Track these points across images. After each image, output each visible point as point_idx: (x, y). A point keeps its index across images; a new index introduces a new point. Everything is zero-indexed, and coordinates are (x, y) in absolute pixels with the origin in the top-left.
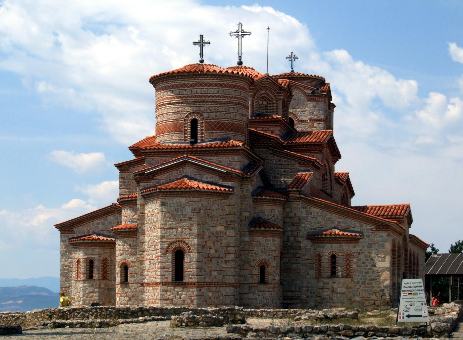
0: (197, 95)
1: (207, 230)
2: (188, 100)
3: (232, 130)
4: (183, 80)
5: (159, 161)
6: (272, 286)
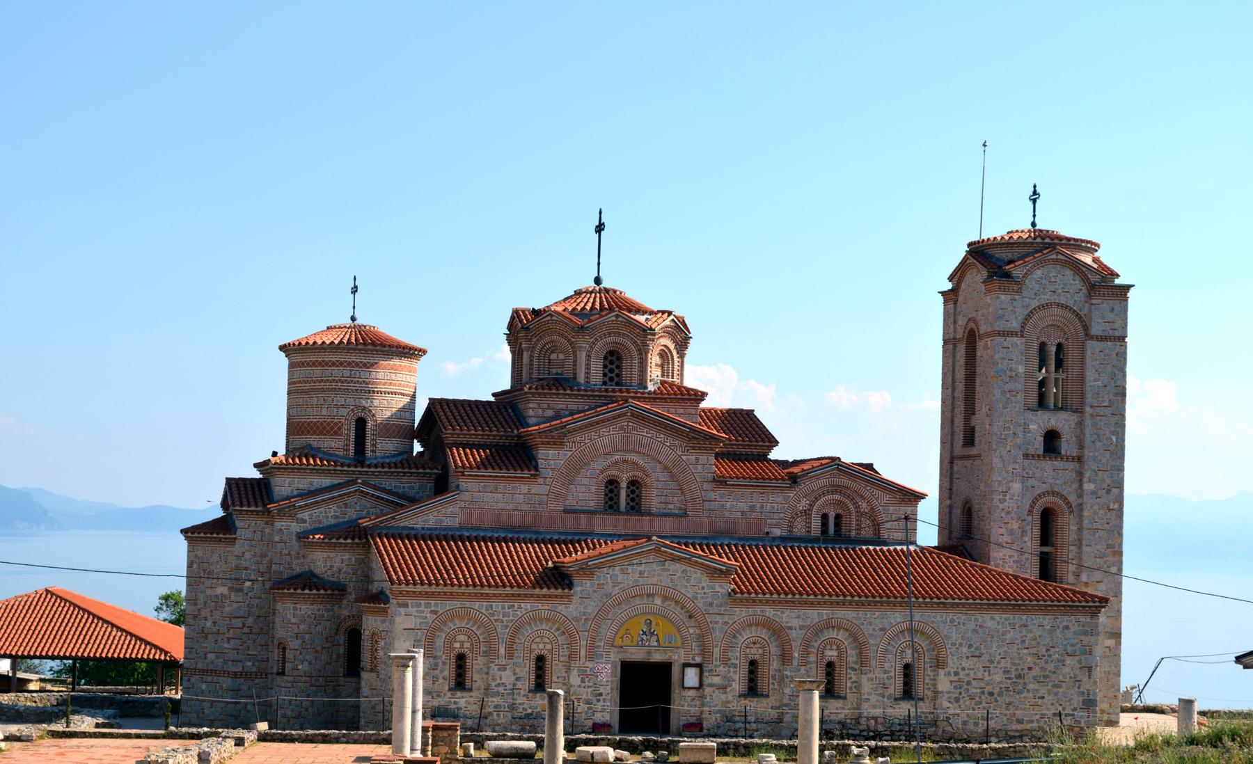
1: (202, 592)
3: (315, 433)
6: (291, 679)
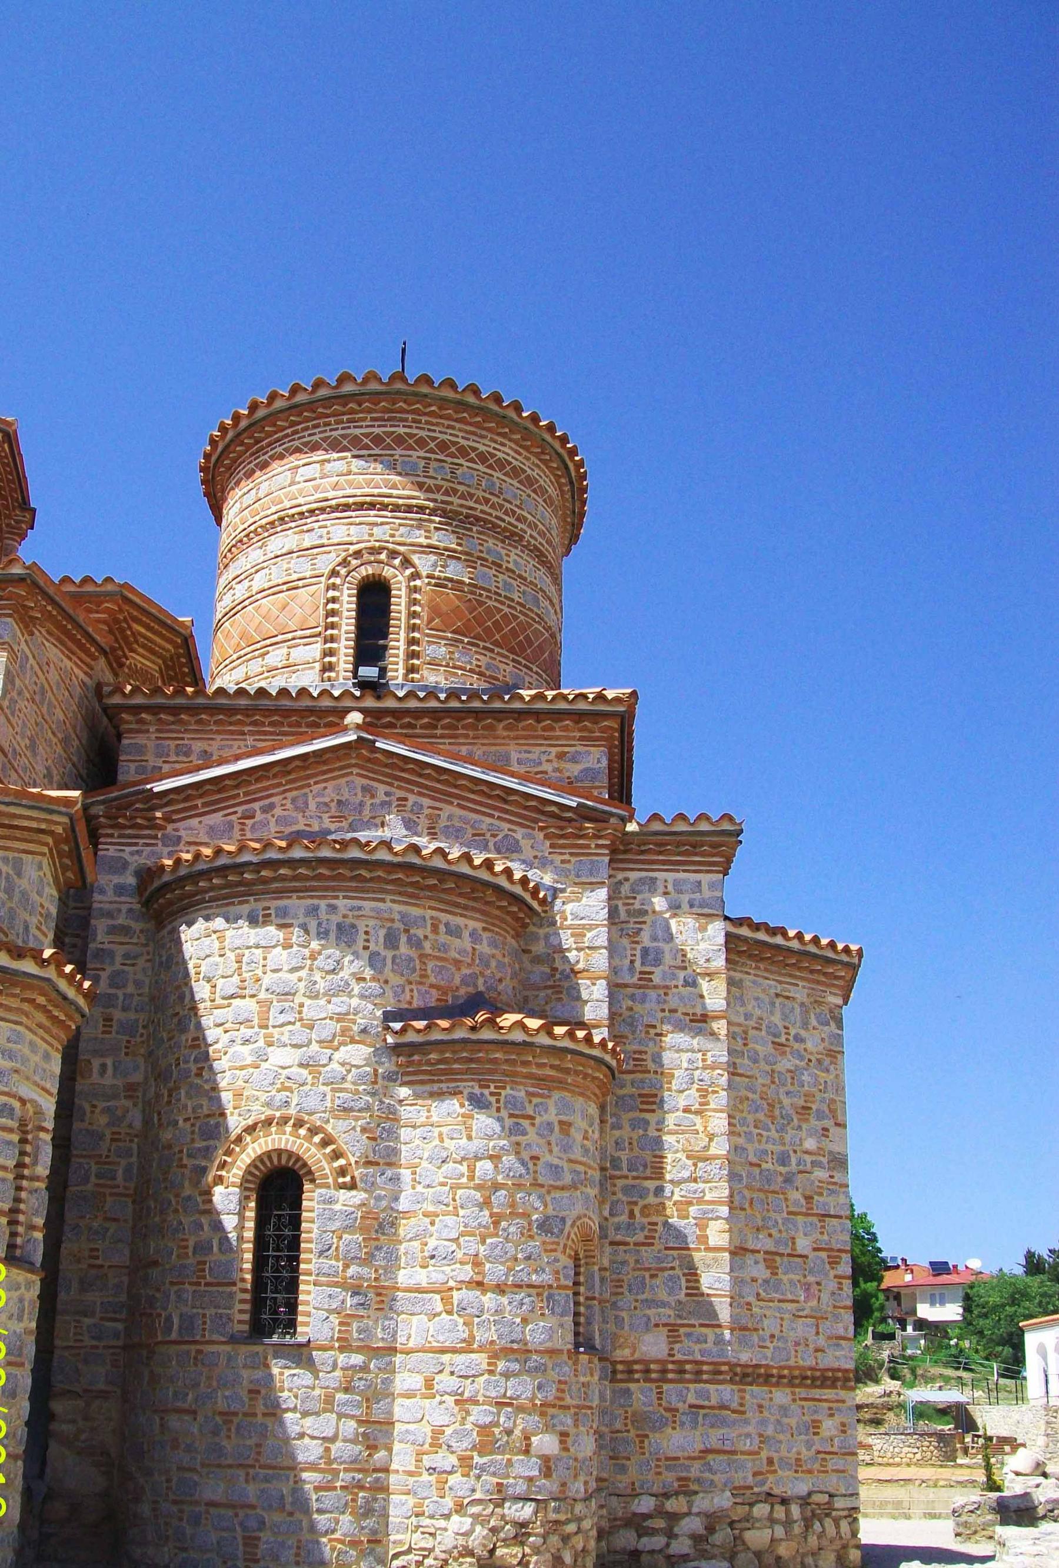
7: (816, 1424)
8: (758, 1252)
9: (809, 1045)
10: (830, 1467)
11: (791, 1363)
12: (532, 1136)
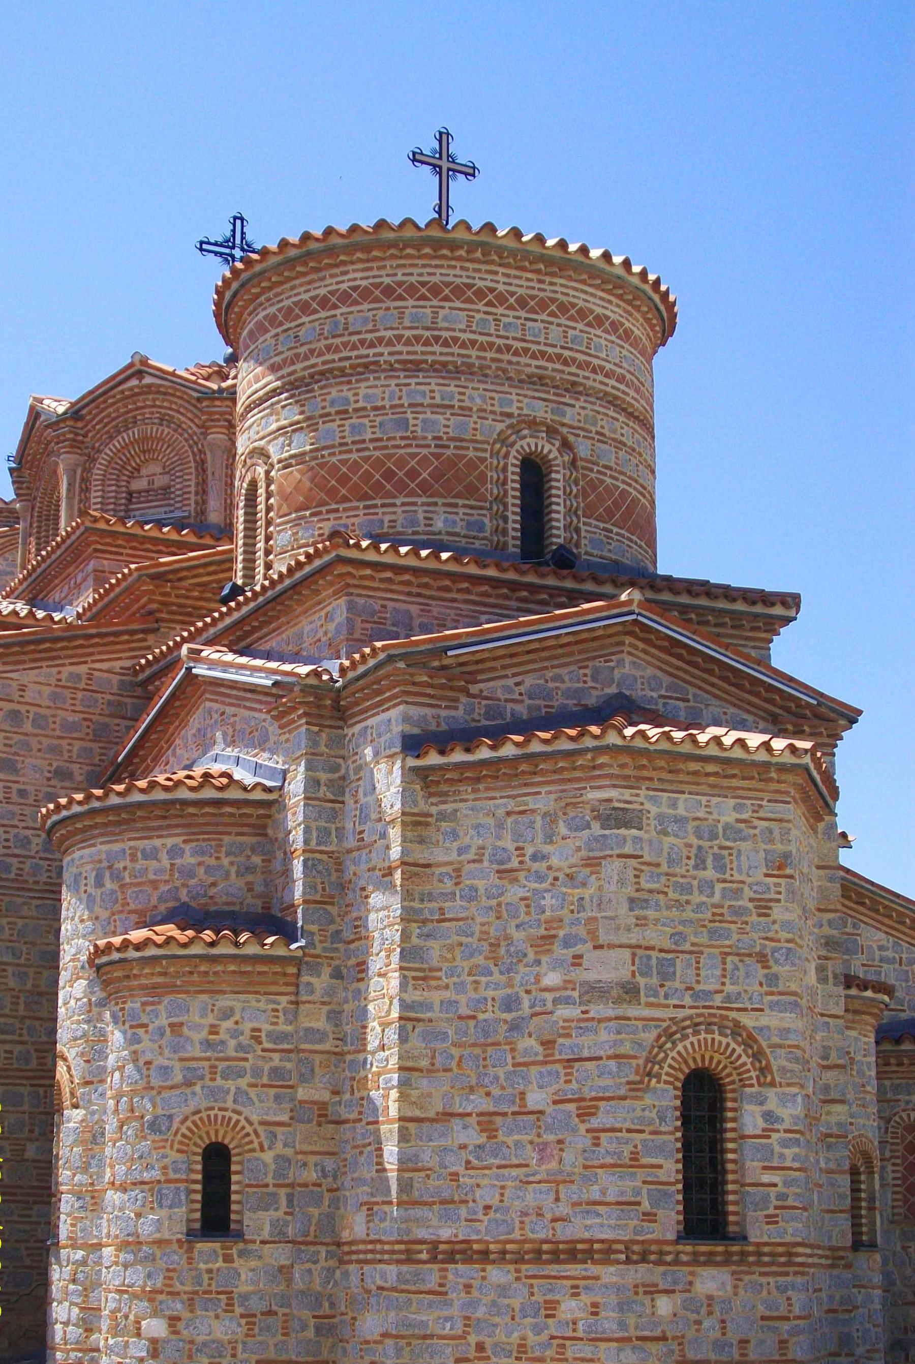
0: (550, 350)
2: (510, 362)
4: (487, 272)
5: (411, 618)
7: (551, 1308)
8: (469, 1115)
9: (555, 861)
10: (569, 1354)
11: (516, 1235)
12: (146, 1044)
